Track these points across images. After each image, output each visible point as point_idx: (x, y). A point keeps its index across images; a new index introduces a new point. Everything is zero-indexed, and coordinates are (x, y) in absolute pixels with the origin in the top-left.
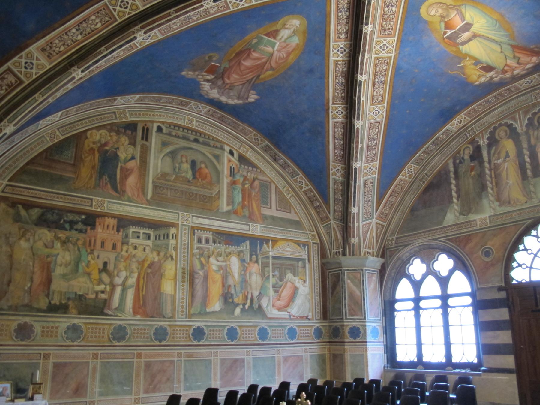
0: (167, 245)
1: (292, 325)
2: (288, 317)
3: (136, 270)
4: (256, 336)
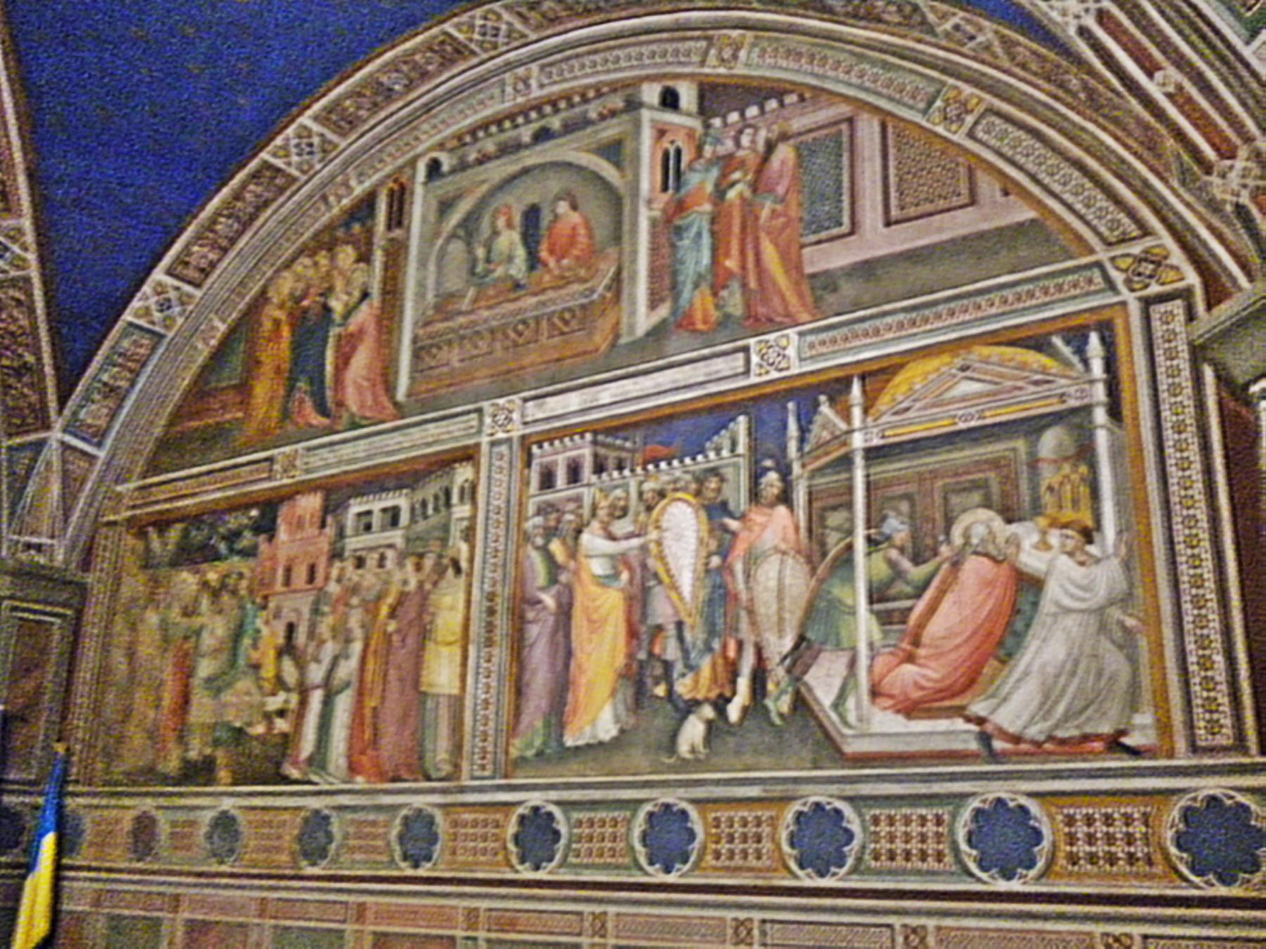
0: (446, 528)
1: (998, 790)
2: (974, 746)
3: (358, 633)
4: (779, 848)
